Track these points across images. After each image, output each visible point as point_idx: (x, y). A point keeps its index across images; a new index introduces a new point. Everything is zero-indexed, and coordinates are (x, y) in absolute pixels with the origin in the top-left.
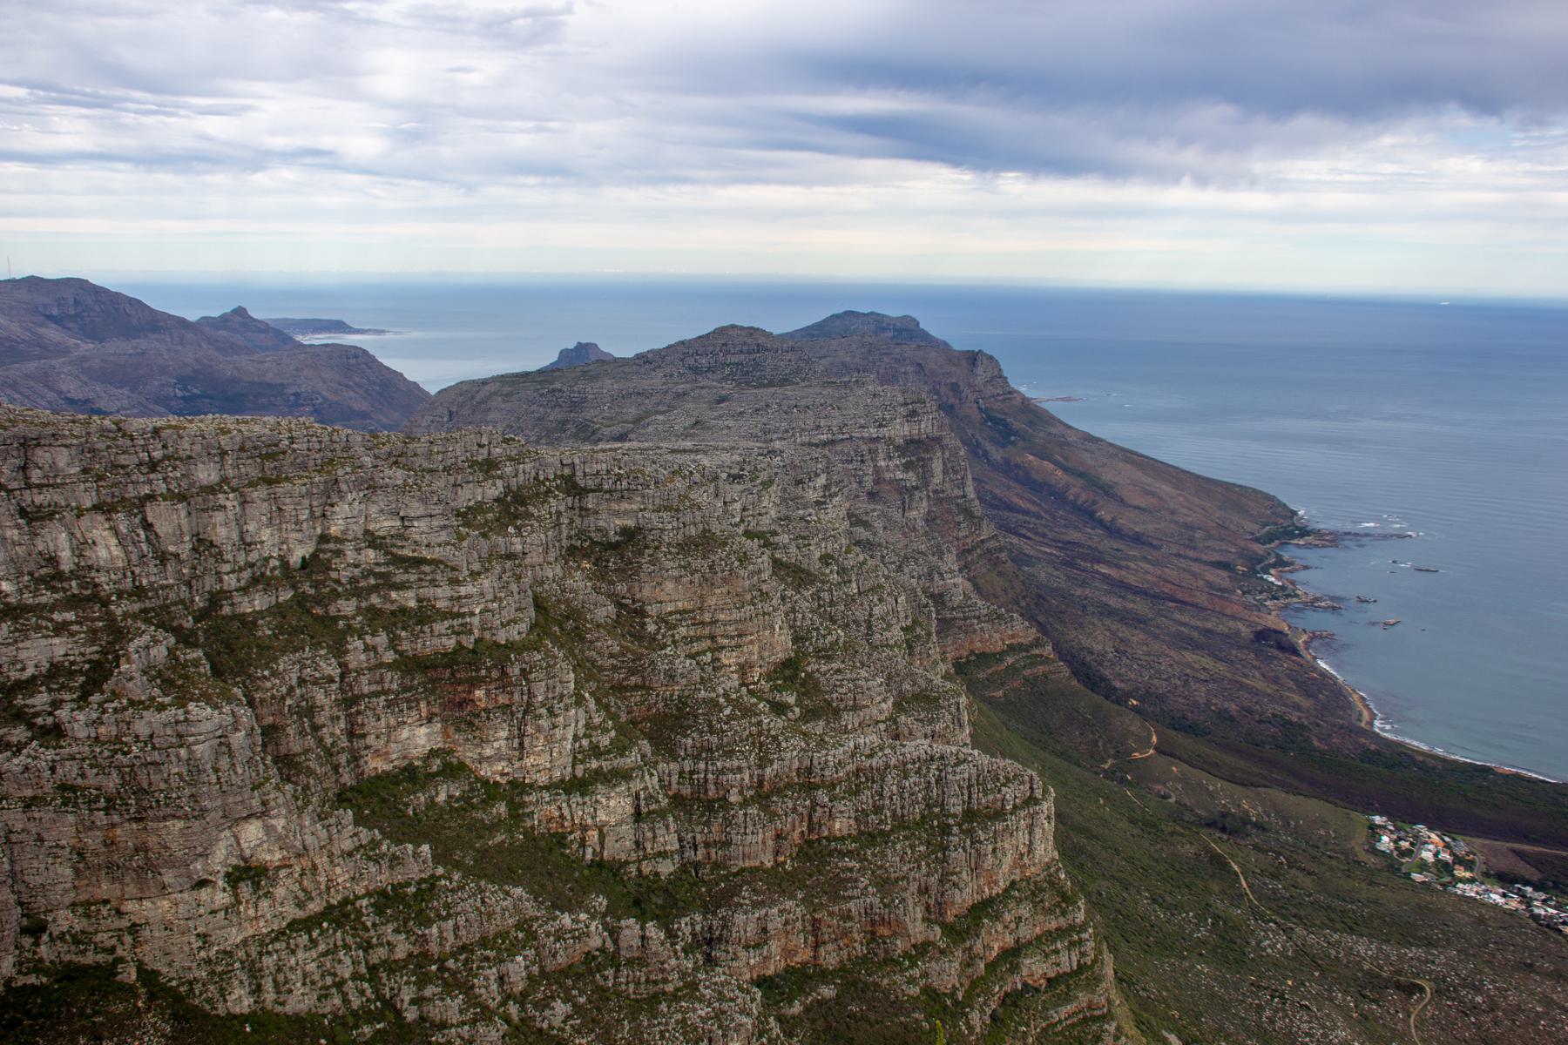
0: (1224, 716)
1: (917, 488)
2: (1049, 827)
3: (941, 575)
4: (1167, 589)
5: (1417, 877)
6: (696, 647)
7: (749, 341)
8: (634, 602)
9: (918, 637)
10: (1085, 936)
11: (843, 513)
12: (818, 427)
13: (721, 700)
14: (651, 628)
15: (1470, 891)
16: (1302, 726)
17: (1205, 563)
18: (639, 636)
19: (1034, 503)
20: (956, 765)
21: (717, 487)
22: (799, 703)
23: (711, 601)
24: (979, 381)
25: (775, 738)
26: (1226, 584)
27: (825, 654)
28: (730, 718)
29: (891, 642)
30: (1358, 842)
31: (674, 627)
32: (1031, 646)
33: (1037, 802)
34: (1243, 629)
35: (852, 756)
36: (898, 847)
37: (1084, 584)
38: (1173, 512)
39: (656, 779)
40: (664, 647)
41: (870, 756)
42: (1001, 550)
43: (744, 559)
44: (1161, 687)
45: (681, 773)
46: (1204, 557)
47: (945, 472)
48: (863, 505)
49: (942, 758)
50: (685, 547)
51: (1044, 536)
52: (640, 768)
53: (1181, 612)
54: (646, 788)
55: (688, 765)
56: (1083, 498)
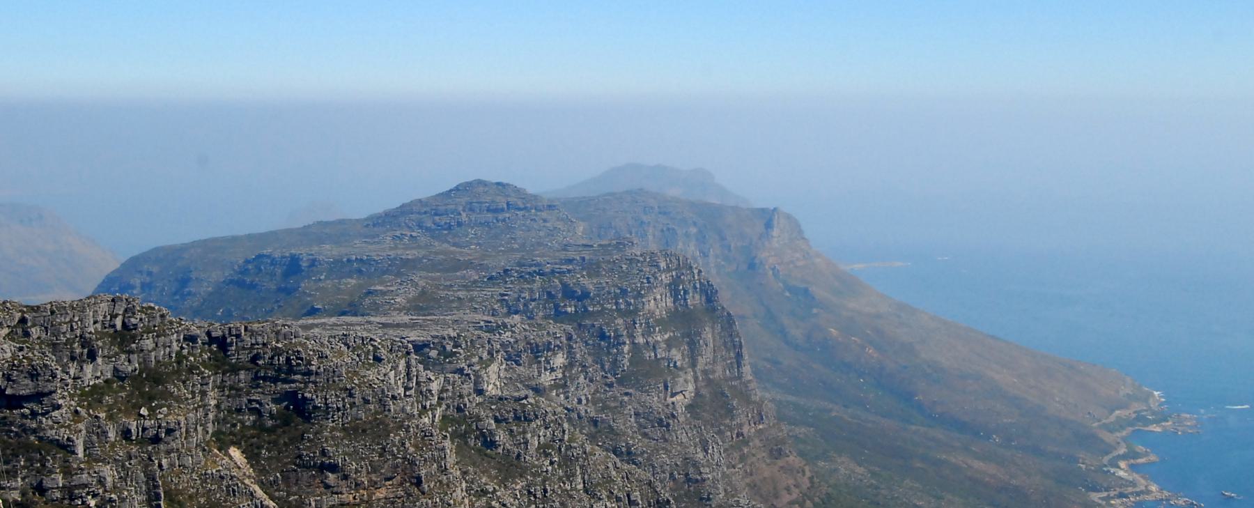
1: (681, 369)
21: (408, 366)
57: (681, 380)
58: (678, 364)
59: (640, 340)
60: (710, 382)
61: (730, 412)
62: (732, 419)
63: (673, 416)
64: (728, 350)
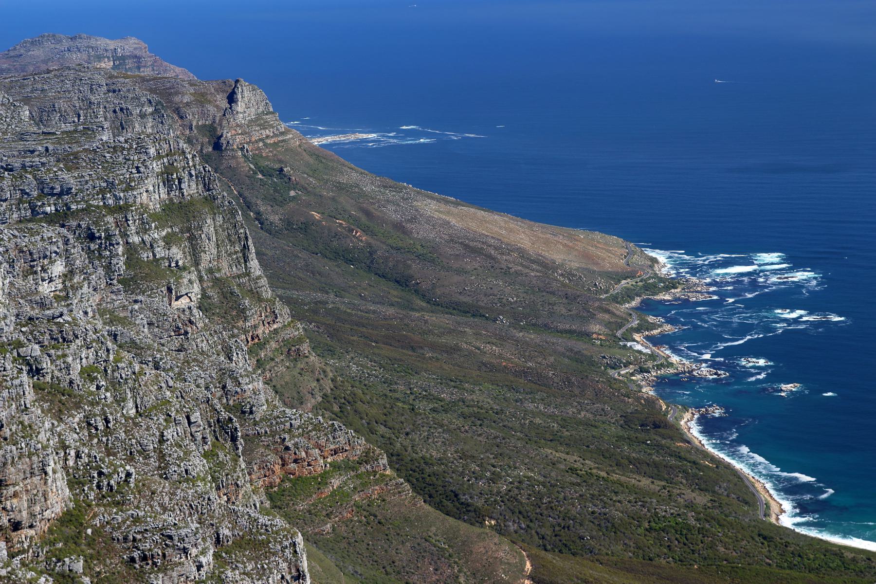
1: (184, 268)
9: (221, 465)
57: (185, 281)
58: (180, 263)
59: (136, 239)
60: (217, 282)
61: (242, 313)
62: (246, 319)
63: (191, 322)
64: (232, 243)
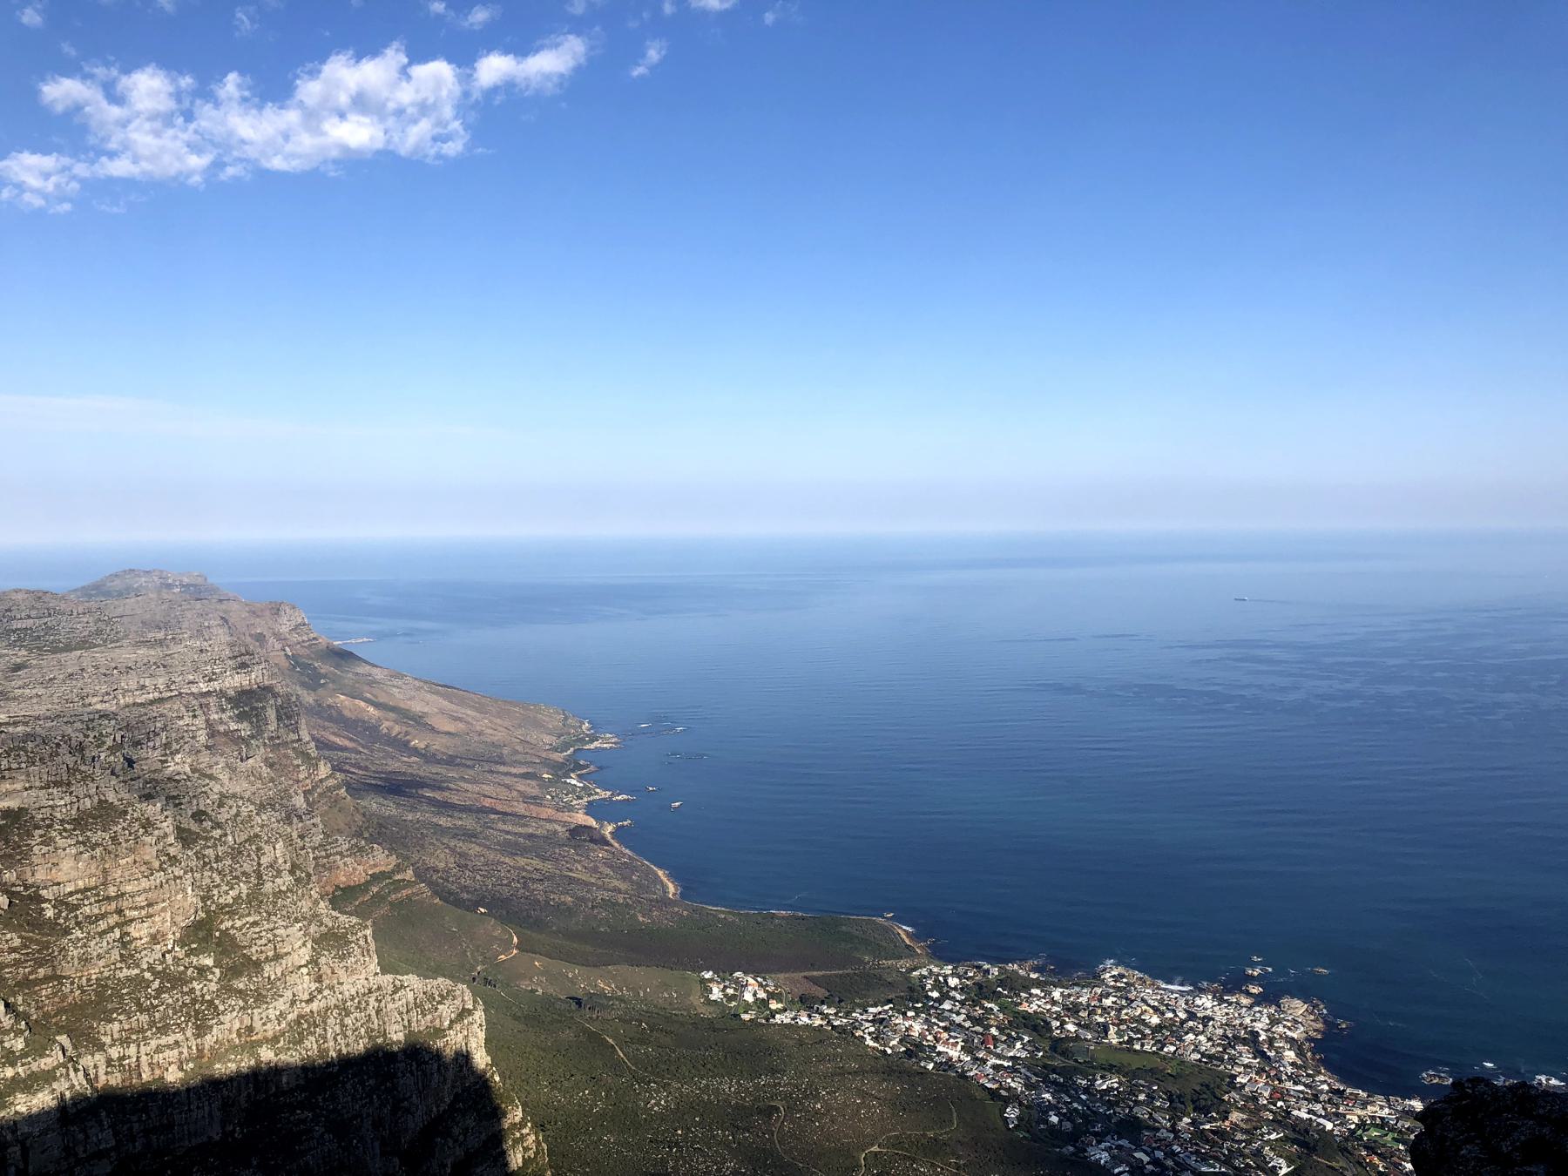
0: (559, 909)
1: (252, 737)
2: (482, 1035)
3: (300, 817)
4: (487, 803)
5: (746, 1017)
6: (103, 925)
7: (38, 605)
8: (26, 887)
10: (525, 1131)
11: (188, 769)
12: (143, 687)
13: (147, 975)
14: (50, 913)
15: (783, 1019)
16: (627, 905)
17: (515, 775)
18: (38, 924)
19: (351, 740)
20: (394, 992)
22: (217, 964)
23: (117, 874)
24: (284, 629)
25: (211, 1002)
26: (535, 792)
27: (230, 911)
28: (159, 991)
29: (284, 888)
30: (696, 1000)
31: (76, 907)
32: (393, 872)
33: (470, 1012)
34: (559, 828)
35: (293, 1003)
36: (348, 1086)
37: (413, 809)
38: (480, 734)
39: (81, 1074)
40: (67, 932)
41: (310, 1001)
42: (338, 787)
43: (148, 825)
44: (506, 892)
45: (109, 1062)
46: (514, 771)
47: (279, 719)
48: (205, 758)
49: (379, 988)
50: (80, 822)
51: (366, 768)
52: (64, 1065)
53: (504, 822)
54: (73, 1086)
55: (114, 1053)
56: (397, 729)
